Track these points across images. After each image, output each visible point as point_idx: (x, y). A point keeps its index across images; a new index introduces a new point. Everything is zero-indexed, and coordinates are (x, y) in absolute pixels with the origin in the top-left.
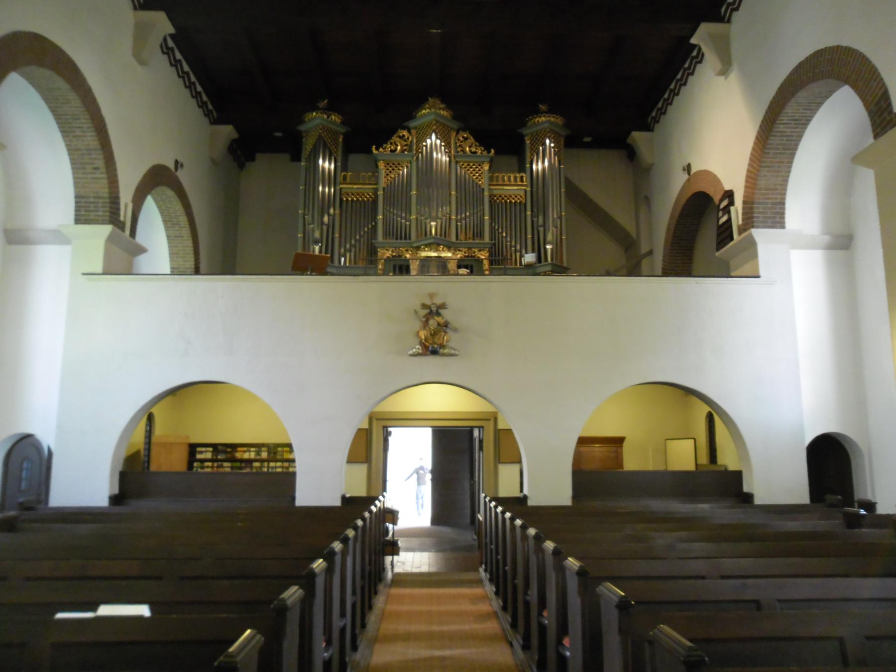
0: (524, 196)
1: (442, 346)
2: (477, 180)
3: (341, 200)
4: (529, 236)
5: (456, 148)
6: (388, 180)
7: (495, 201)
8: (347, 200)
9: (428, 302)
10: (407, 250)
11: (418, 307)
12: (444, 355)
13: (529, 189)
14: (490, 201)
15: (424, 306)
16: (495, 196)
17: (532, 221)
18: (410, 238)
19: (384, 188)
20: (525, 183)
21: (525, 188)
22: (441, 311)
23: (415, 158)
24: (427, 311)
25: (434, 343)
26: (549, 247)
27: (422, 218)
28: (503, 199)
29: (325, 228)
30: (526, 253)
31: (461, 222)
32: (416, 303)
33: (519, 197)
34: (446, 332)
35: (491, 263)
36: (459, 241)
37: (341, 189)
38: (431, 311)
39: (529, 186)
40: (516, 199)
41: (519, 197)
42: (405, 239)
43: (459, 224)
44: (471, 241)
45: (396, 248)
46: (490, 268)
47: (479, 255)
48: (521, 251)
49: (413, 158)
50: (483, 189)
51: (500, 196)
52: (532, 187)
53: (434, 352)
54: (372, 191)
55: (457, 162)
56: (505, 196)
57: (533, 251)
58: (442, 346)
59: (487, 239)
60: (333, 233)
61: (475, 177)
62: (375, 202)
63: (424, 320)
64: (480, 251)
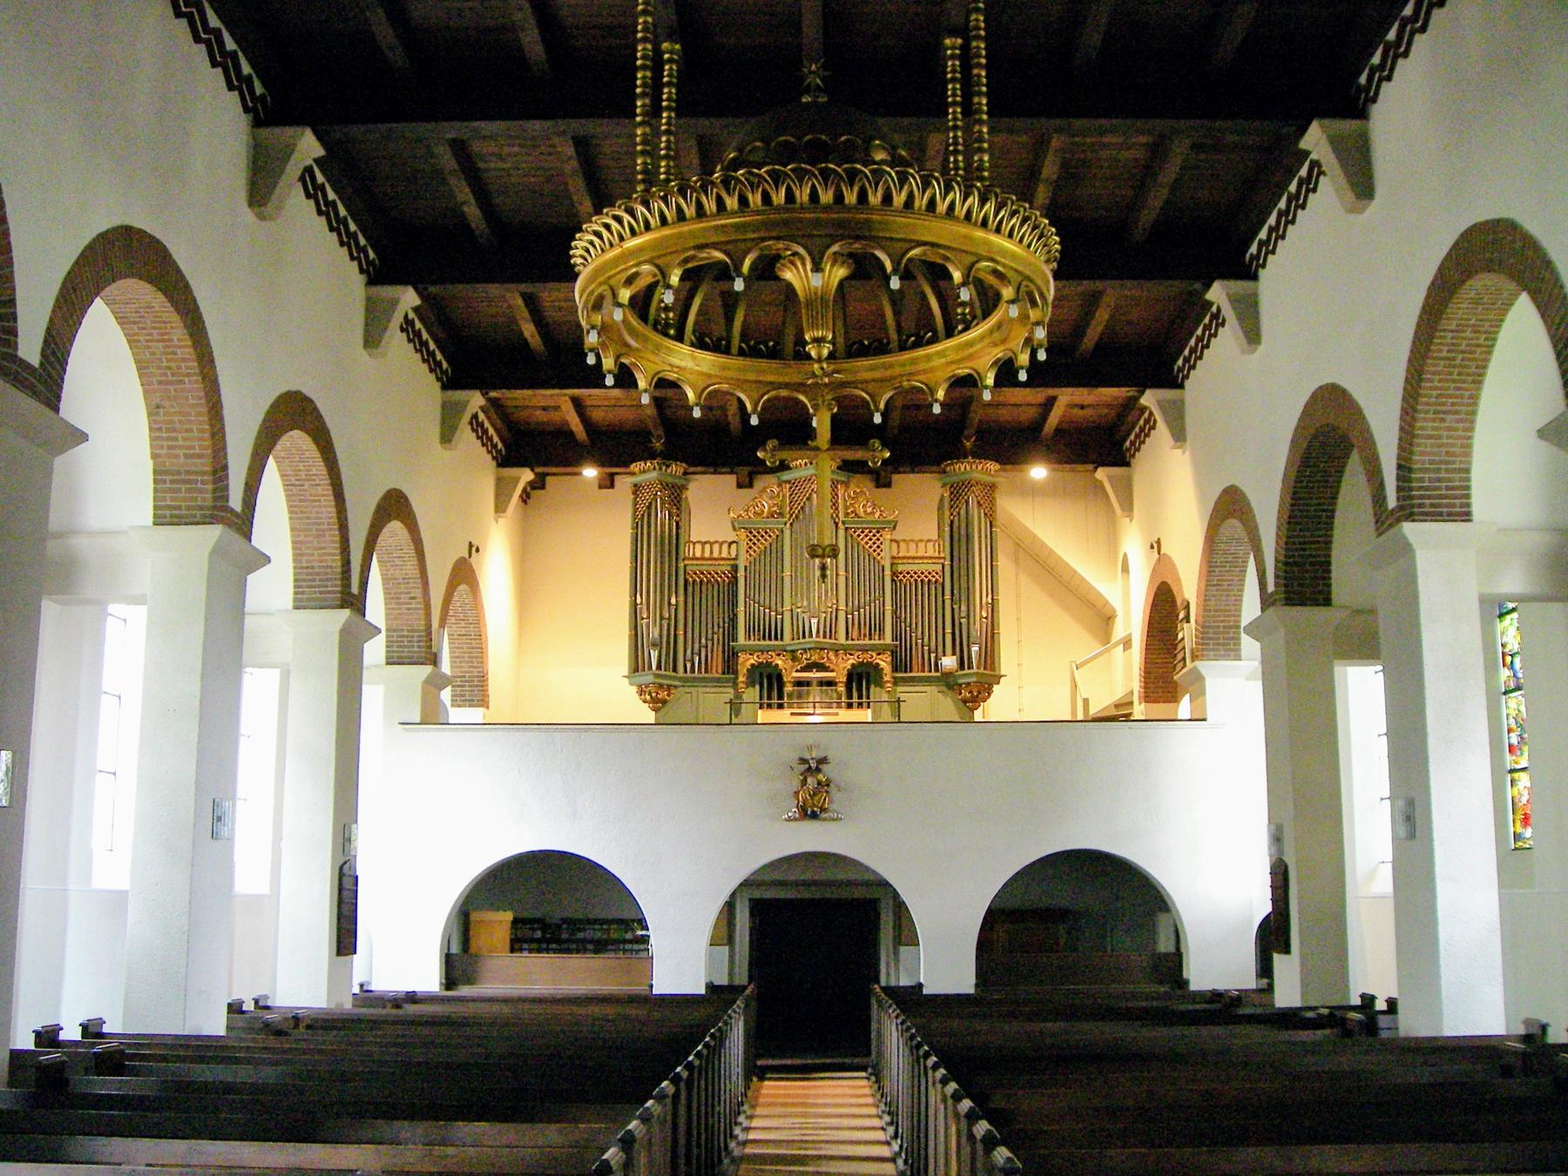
0: (941, 573)
1: (823, 810)
2: (875, 554)
3: (686, 581)
4: (949, 630)
5: (846, 508)
6: (750, 555)
7: (901, 580)
8: (694, 581)
9: (807, 756)
10: (779, 655)
11: (795, 764)
12: (825, 820)
13: (947, 563)
14: (893, 580)
15: (803, 761)
16: (901, 573)
17: (953, 609)
18: (782, 639)
19: (746, 567)
20: (942, 555)
21: (942, 561)
22: (820, 766)
23: (788, 525)
24: (807, 766)
25: (814, 805)
26: (975, 649)
27: (799, 610)
28: (912, 577)
29: (665, 623)
30: (944, 655)
31: (853, 614)
32: (793, 756)
33: (934, 574)
34: (827, 792)
35: (895, 669)
36: (850, 642)
37: (685, 566)
38: (810, 767)
39: (948, 557)
40: (930, 577)
41: (934, 574)
42: (776, 638)
43: (850, 616)
44: (867, 642)
45: (762, 652)
46: (894, 678)
47: (877, 661)
48: (937, 652)
49: (785, 524)
50: (883, 567)
51: (908, 573)
52: (952, 561)
53: (814, 816)
54: (729, 568)
55: (846, 529)
56: (915, 573)
57: (954, 654)
58: (823, 810)
59: (888, 640)
60: (675, 630)
61: (871, 550)
62: (734, 581)
63: (801, 778)
64: (879, 654)
